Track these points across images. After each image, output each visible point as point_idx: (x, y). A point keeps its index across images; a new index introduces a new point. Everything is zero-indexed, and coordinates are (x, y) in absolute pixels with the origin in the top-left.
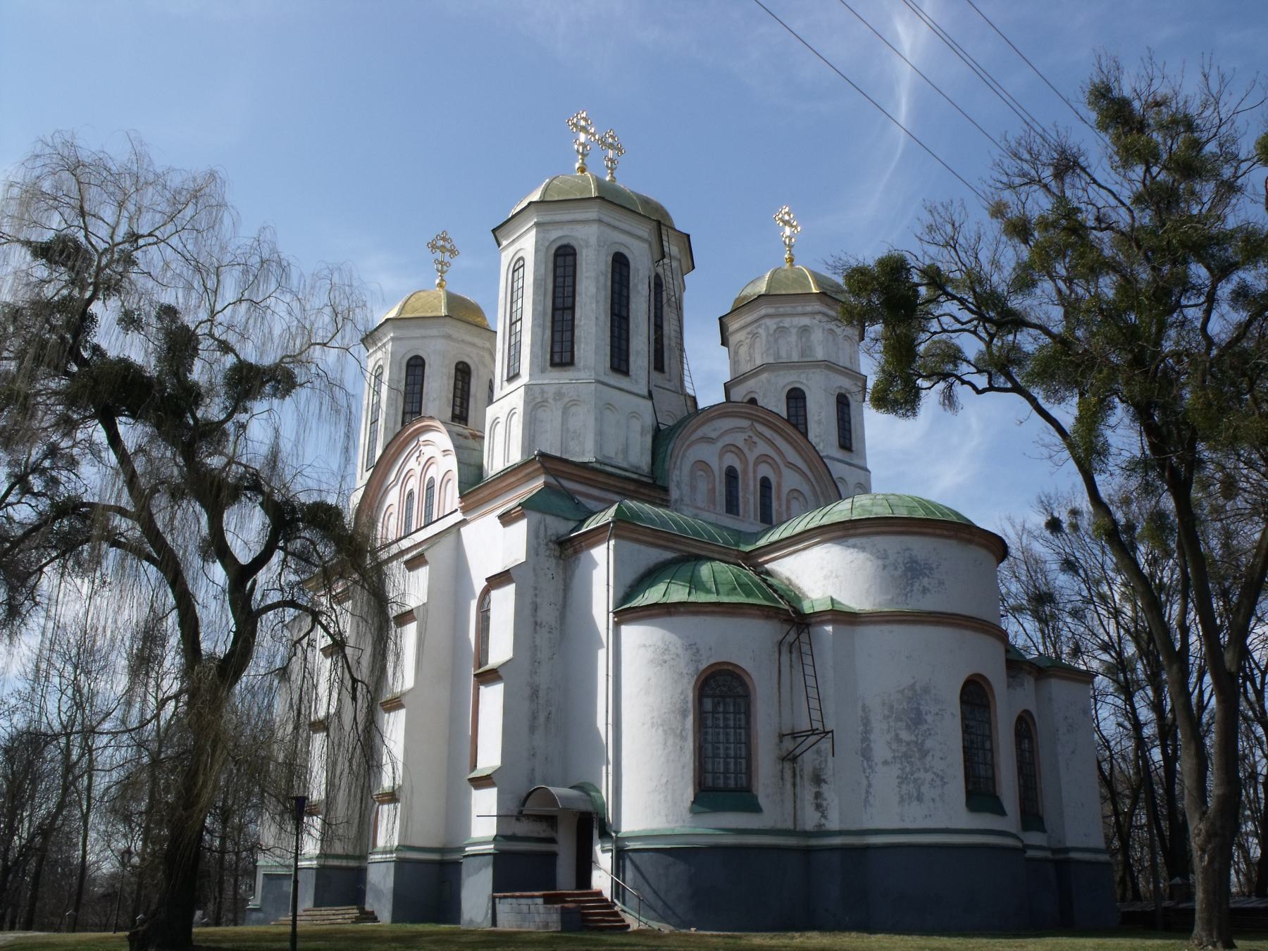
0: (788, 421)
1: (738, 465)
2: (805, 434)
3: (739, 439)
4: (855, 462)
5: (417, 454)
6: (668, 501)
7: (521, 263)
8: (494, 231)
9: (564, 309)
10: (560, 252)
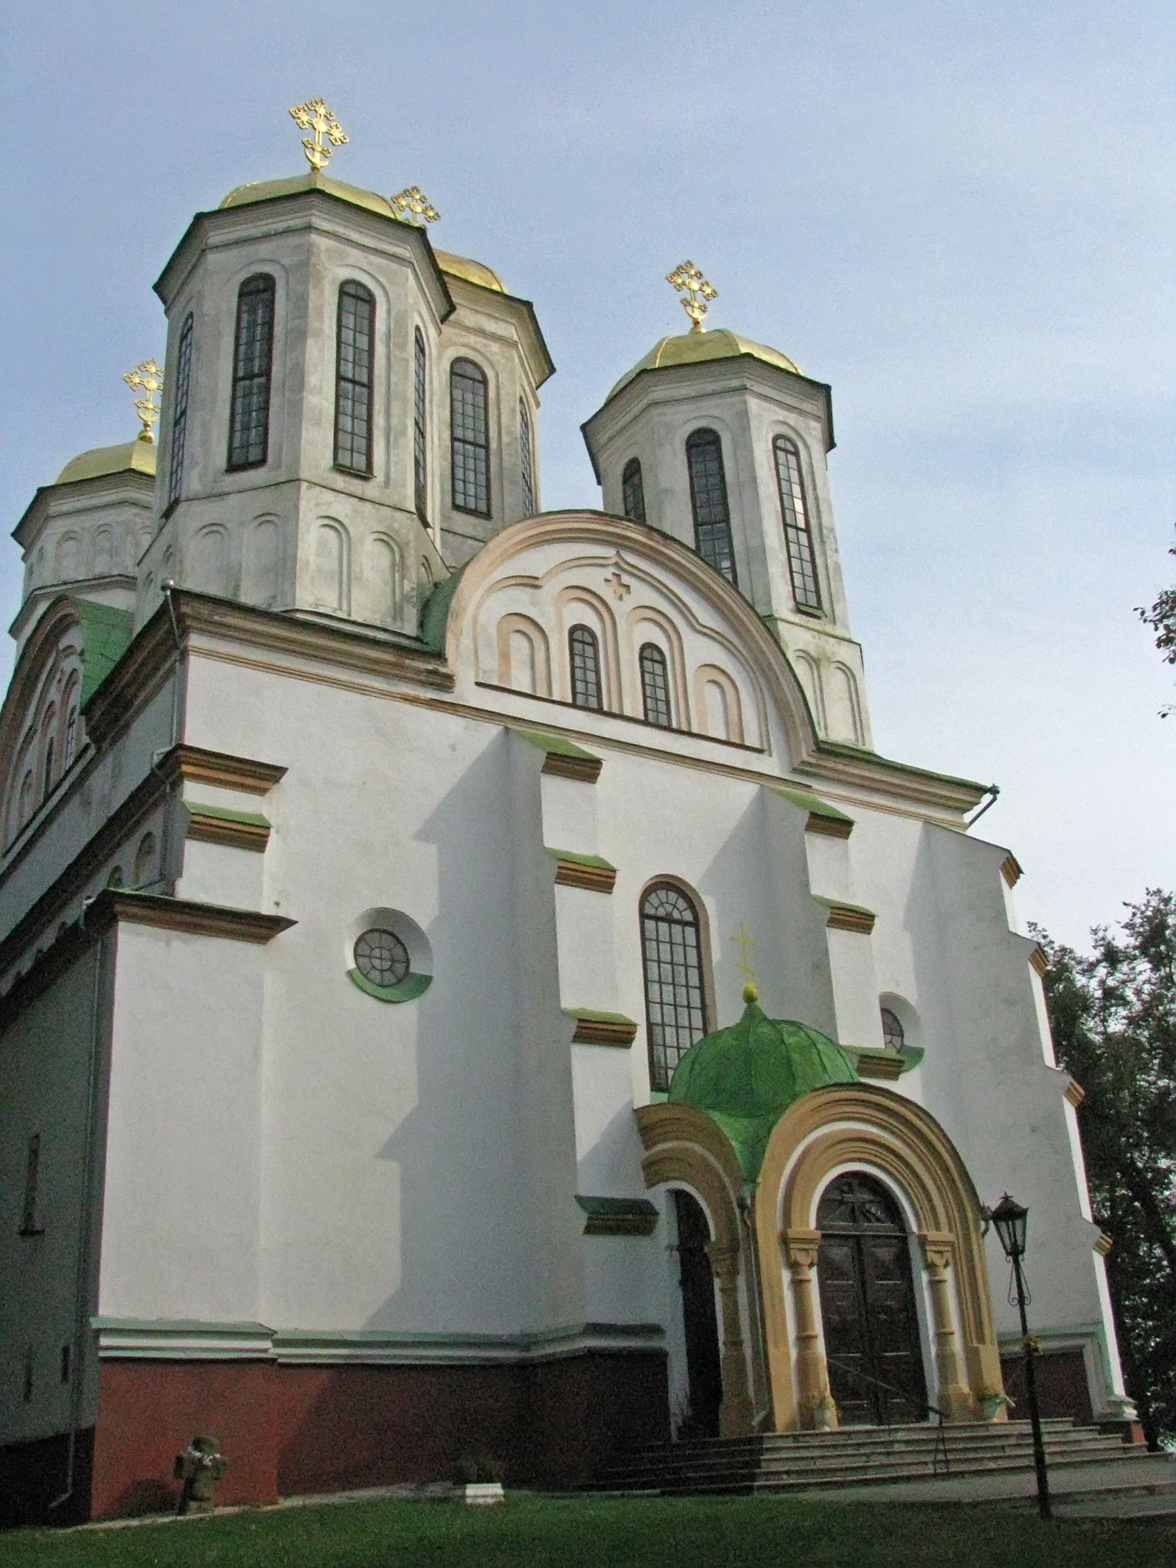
0: (696, 552)
1: (591, 620)
2: (734, 583)
3: (595, 579)
4: (829, 629)
5: (58, 677)
6: (445, 682)
7: (190, 321)
8: (157, 288)
9: (250, 376)
10: (246, 290)
